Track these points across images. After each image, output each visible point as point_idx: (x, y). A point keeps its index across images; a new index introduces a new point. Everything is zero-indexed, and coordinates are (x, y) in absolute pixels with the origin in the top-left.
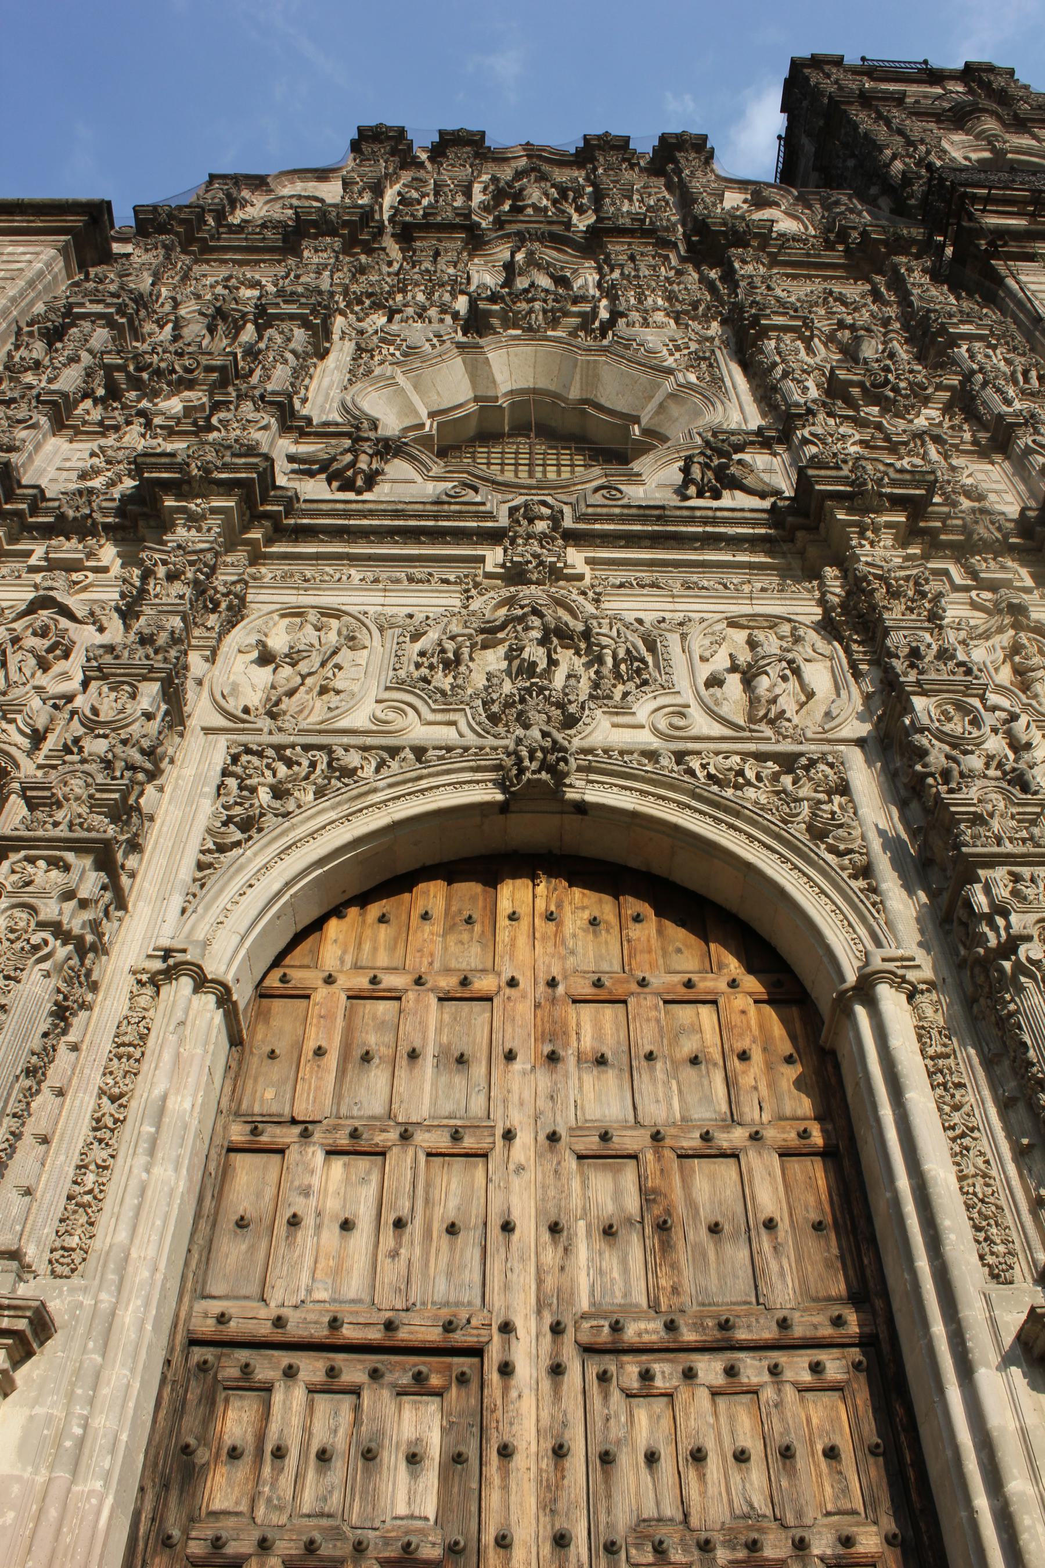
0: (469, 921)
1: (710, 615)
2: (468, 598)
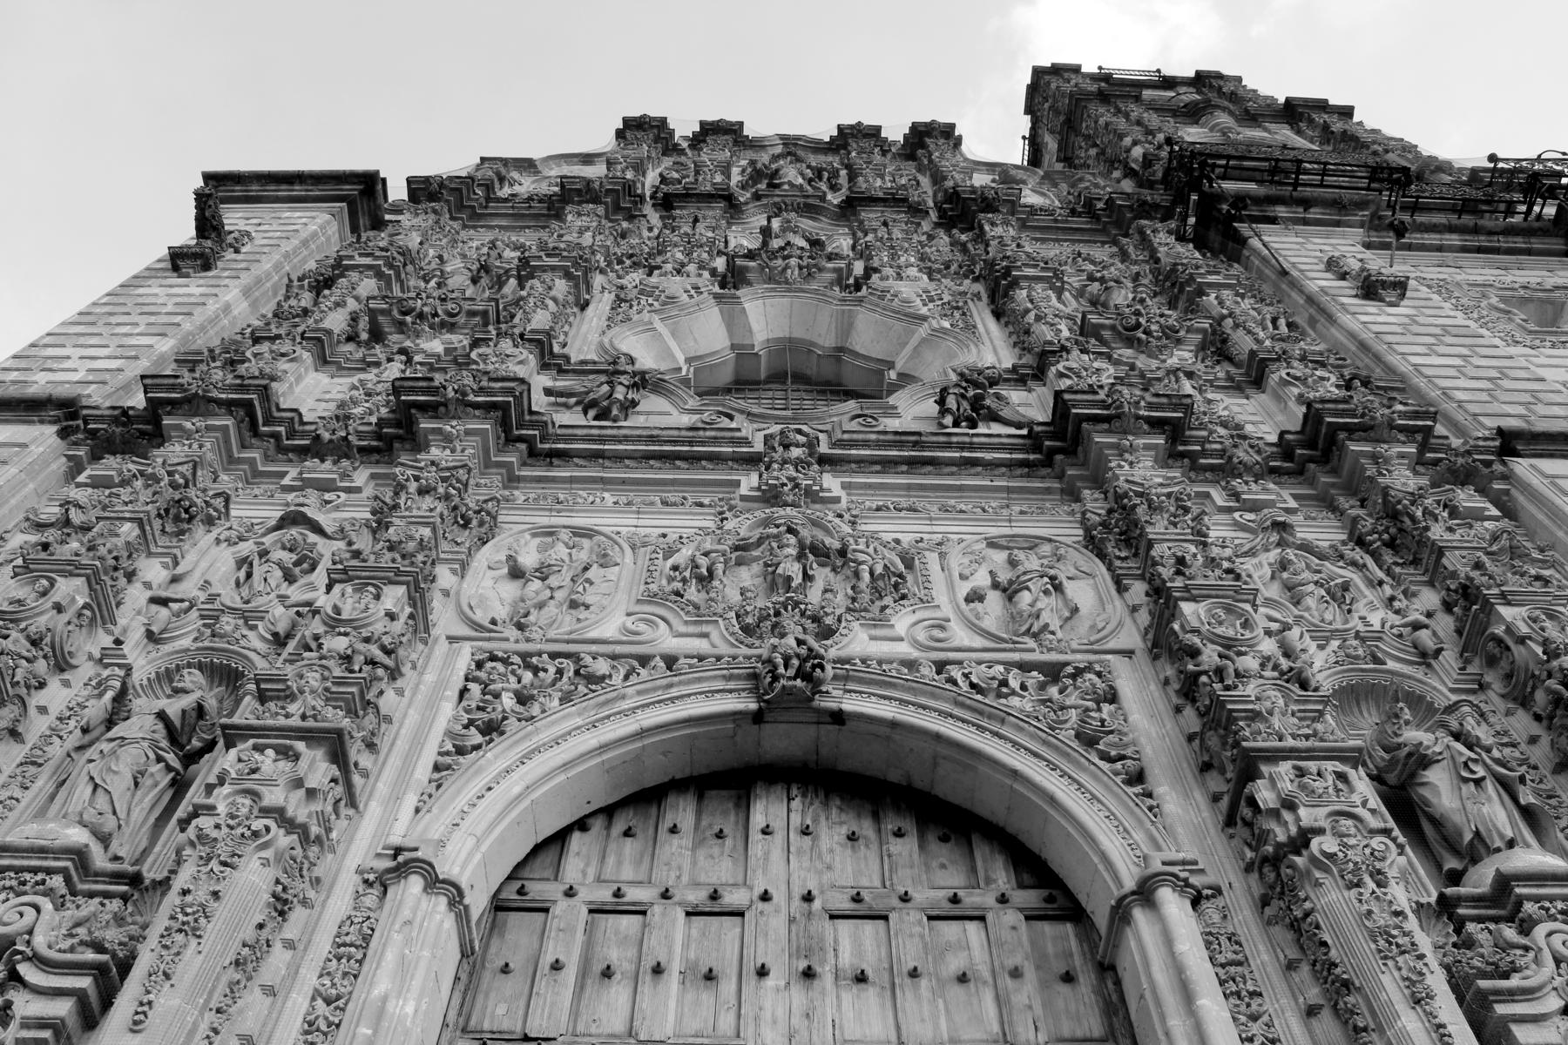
0: (720, 835)
2: (722, 520)
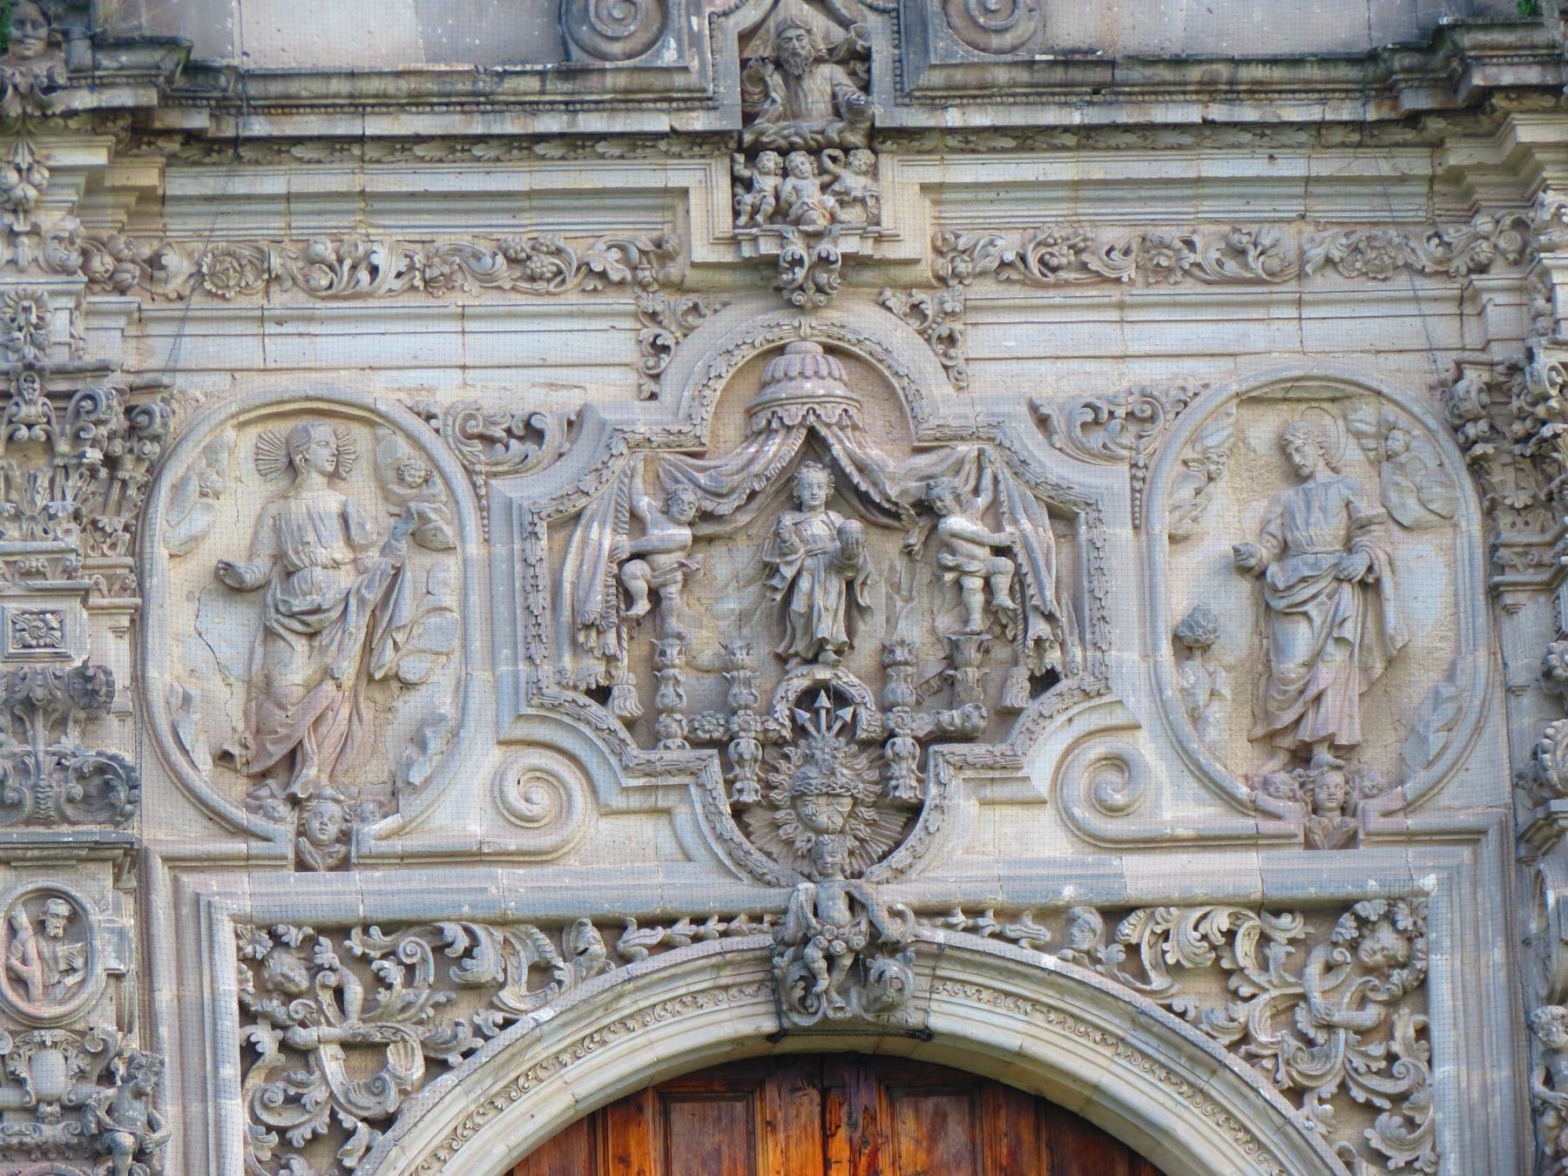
1: (1204, 368)
2: (661, 349)
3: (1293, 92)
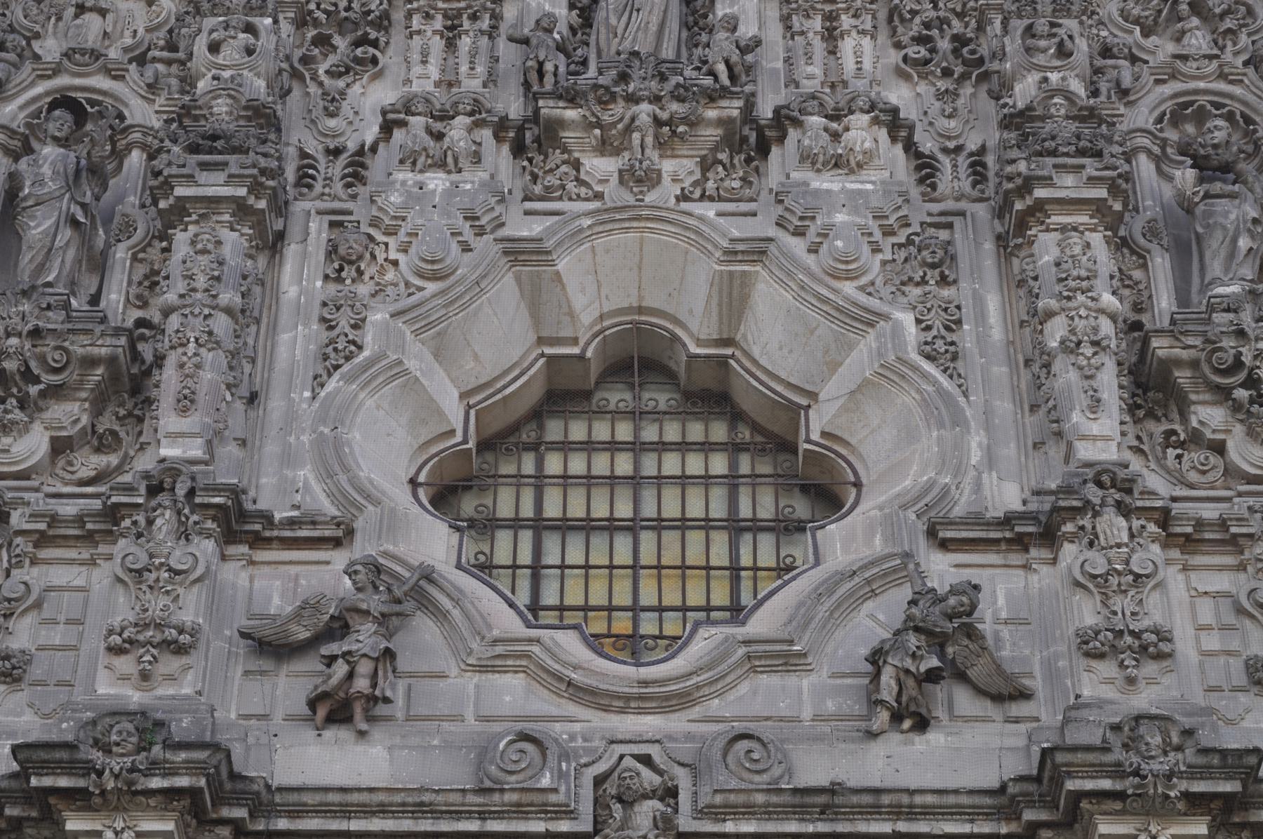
3: (952, 814)
